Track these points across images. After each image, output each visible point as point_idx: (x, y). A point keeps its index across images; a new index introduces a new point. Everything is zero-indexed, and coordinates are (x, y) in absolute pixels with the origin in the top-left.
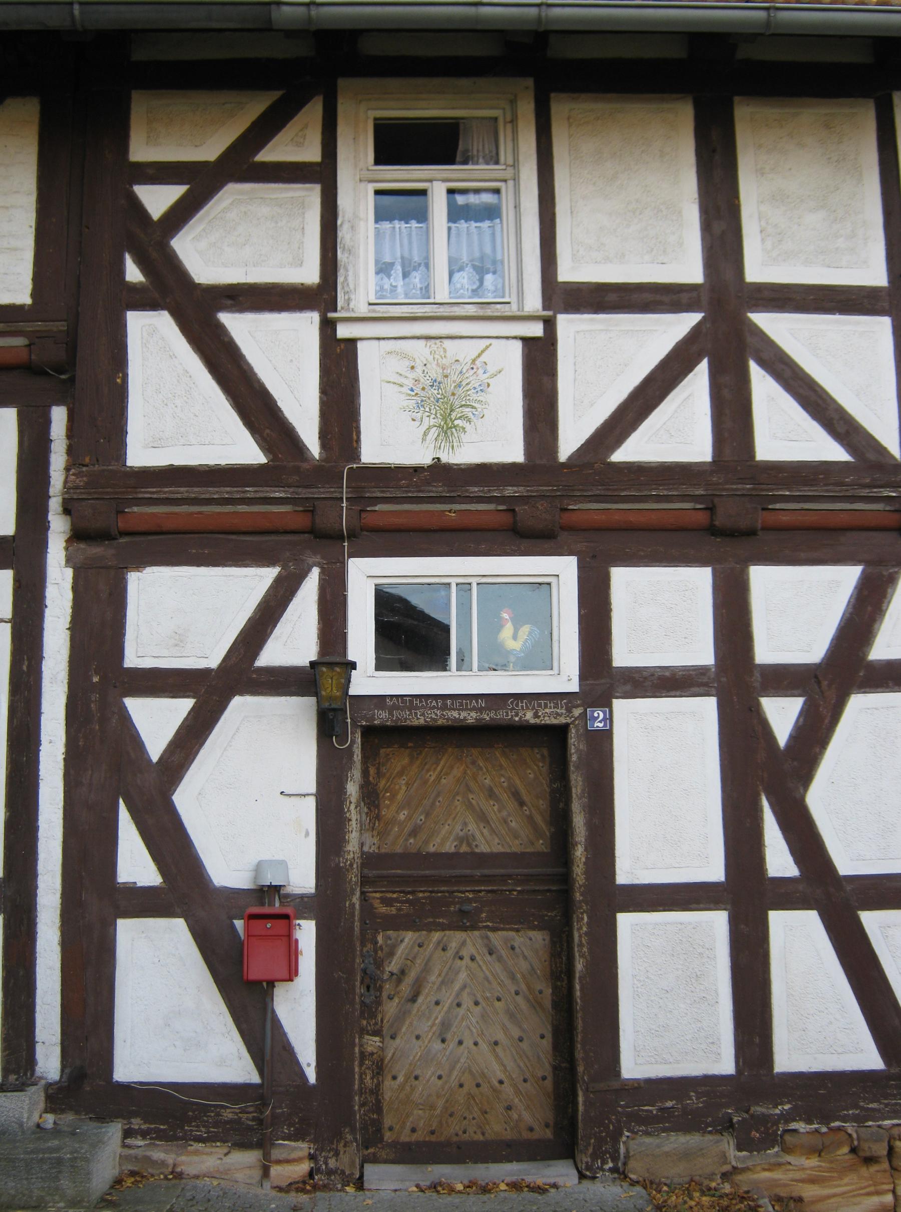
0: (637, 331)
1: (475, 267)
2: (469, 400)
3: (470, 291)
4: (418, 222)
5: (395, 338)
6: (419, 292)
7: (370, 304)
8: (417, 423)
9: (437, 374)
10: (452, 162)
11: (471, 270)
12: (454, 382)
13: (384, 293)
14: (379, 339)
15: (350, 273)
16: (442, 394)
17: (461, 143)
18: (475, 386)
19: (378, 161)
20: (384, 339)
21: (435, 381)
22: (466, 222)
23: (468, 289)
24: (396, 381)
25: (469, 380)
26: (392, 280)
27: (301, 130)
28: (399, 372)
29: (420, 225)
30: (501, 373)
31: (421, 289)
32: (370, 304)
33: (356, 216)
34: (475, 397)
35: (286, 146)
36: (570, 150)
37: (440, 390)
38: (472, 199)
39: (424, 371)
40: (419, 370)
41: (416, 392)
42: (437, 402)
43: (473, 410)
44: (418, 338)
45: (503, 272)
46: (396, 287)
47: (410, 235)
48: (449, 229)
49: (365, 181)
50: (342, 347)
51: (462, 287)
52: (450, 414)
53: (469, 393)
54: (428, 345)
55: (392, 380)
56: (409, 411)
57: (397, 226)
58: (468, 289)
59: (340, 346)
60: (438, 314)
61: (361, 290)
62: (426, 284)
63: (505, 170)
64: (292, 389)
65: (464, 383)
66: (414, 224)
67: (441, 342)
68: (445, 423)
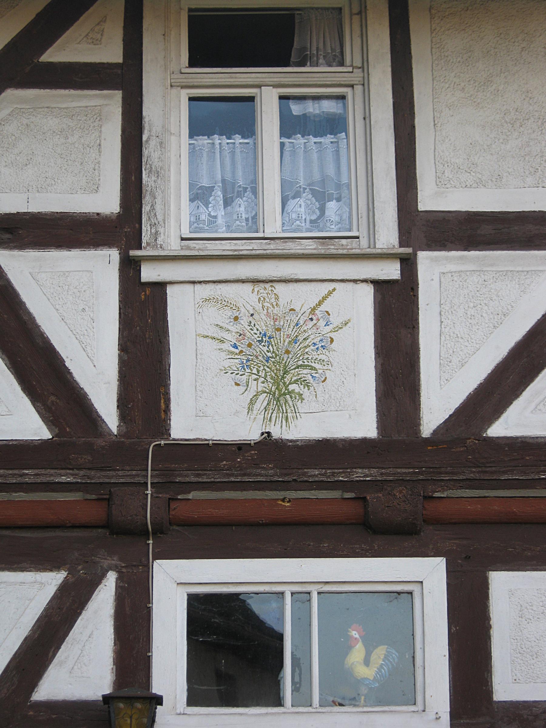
0: (518, 272)
1: (314, 192)
2: (307, 358)
3: (308, 222)
4: (243, 137)
5: (214, 282)
6: (244, 224)
7: (183, 239)
8: (242, 389)
9: (267, 326)
10: (287, 64)
11: (310, 196)
12: (288, 336)
13: (201, 225)
14: (194, 282)
15: (158, 201)
16: (273, 352)
17: (296, 39)
18: (315, 341)
19: (192, 63)
20: (200, 282)
21: (265, 335)
22: (303, 136)
23: (305, 219)
24: (215, 335)
25: (307, 334)
26: (210, 209)
27: (98, 24)
28: (219, 323)
29: (246, 141)
30: (348, 325)
31: (247, 220)
32: (183, 239)
33: (165, 129)
34: (315, 355)
35: (79, 43)
36: (432, 48)
37: (270, 347)
38: (311, 108)
39: (250, 322)
40: (244, 321)
41: (240, 348)
42: (267, 361)
43: (313, 372)
44: (243, 281)
45: (351, 199)
46: (215, 217)
47: (233, 153)
48: (282, 145)
49: (178, 86)
50: (148, 292)
51: (299, 218)
52: (283, 378)
53: (306, 350)
54: (256, 290)
55: (210, 334)
56: (232, 373)
57: (217, 142)
58: (305, 219)
59: (145, 292)
60: (268, 252)
61: (172, 222)
62: (254, 213)
63: (352, 72)
64: (83, 345)
65: (301, 338)
66: (238, 139)
67: (271, 286)
68: (277, 388)
